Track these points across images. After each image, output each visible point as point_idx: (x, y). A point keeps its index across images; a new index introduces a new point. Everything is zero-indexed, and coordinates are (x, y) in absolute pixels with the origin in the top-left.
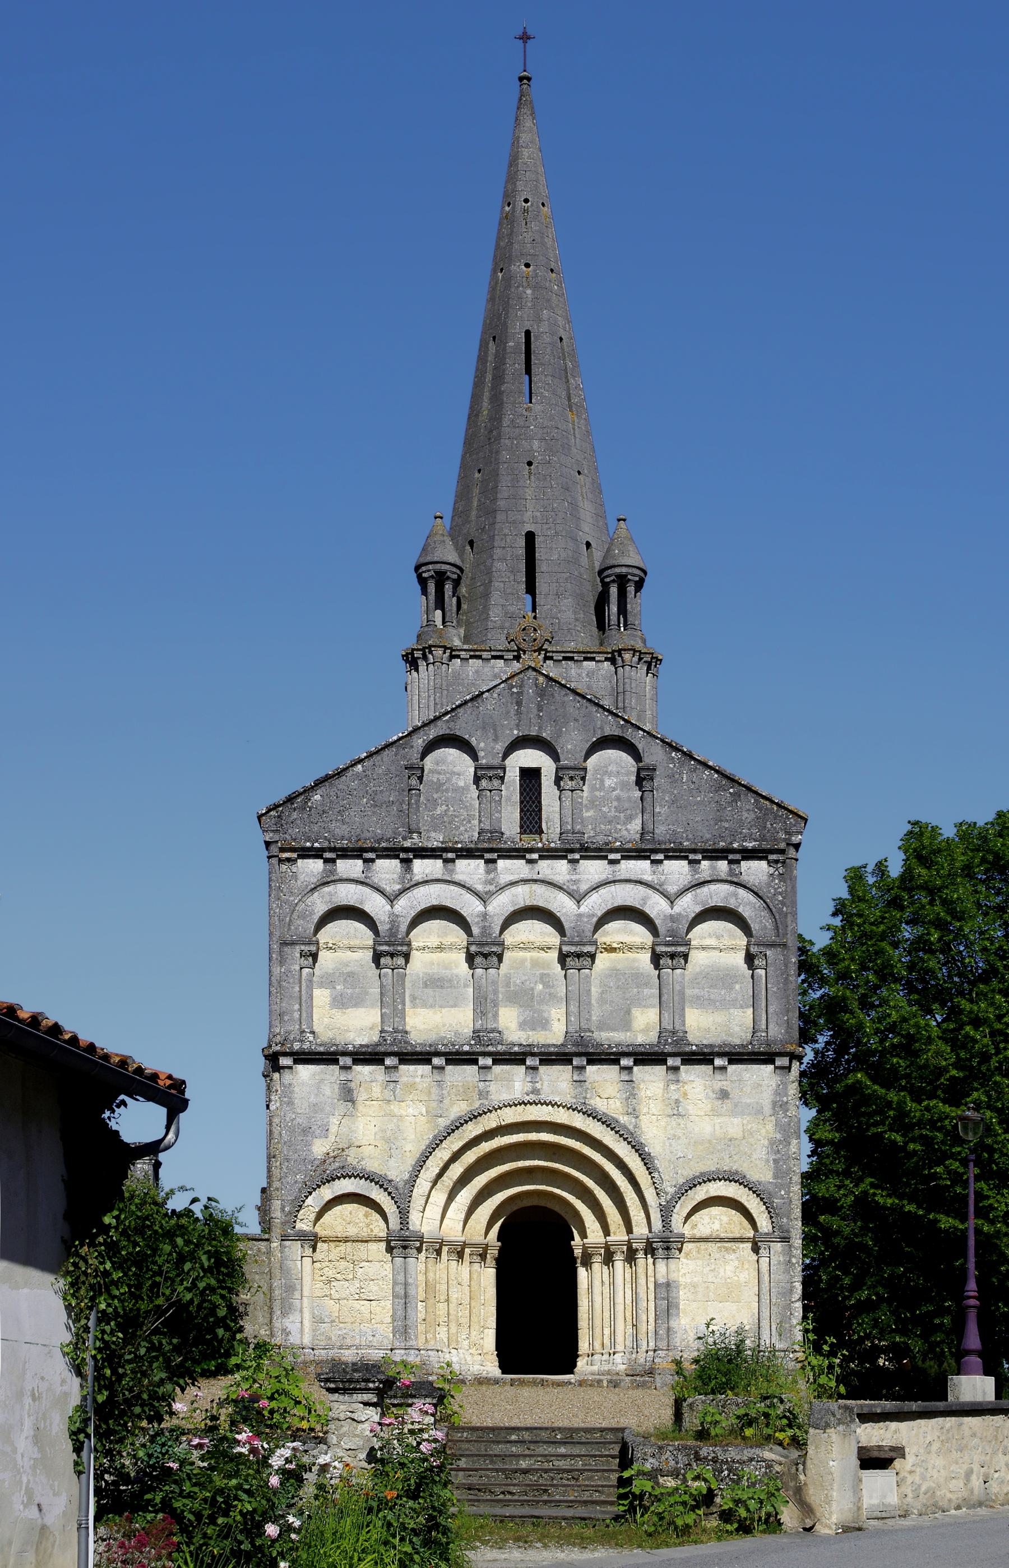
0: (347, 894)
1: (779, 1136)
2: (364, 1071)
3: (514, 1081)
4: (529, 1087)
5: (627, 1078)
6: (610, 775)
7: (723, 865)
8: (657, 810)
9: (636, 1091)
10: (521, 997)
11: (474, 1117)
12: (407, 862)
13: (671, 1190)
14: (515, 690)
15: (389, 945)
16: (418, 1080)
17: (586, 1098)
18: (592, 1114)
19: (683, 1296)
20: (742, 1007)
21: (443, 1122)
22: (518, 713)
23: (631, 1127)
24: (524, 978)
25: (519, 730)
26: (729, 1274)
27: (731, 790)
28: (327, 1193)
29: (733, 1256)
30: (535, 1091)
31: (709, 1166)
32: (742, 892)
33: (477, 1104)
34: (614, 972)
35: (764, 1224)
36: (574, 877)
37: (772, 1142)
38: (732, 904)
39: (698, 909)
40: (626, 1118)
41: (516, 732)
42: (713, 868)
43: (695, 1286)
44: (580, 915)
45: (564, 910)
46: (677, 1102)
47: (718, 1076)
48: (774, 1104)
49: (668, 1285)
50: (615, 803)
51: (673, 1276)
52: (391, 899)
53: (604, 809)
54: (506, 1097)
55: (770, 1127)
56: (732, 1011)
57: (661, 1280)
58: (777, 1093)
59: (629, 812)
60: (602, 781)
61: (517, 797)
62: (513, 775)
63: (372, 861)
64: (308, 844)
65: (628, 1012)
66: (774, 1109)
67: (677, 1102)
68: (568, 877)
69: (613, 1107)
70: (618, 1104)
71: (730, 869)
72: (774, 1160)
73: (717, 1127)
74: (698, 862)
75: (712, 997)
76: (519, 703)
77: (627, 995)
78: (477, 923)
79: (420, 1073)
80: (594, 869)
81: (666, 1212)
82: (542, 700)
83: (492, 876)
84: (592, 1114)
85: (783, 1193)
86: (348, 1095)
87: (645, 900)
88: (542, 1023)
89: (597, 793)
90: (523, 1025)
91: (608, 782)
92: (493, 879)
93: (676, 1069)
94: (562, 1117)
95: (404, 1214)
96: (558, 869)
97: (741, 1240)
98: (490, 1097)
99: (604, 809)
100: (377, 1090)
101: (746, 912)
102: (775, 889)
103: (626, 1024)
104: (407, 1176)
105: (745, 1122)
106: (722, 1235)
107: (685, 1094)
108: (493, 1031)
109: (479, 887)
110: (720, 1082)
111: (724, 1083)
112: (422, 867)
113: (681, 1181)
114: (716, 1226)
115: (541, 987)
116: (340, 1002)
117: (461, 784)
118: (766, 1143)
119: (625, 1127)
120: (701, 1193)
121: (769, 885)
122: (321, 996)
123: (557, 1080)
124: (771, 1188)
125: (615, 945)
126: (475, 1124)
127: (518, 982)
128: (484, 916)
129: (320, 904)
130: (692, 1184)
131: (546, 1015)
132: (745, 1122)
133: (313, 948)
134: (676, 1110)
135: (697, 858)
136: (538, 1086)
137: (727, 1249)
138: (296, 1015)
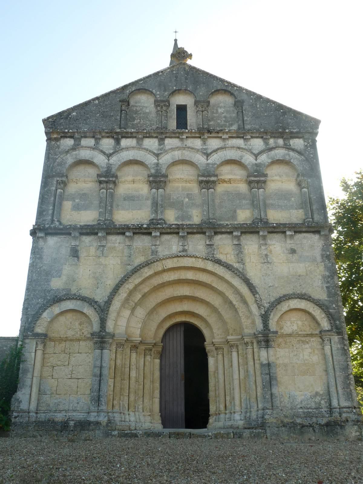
0: (84, 154)
1: (327, 274)
2: (87, 240)
3: (171, 245)
4: (181, 248)
5: (237, 243)
6: (221, 107)
7: (281, 142)
8: (245, 118)
9: (242, 250)
10: (177, 205)
11: (147, 264)
12: (118, 141)
13: (267, 305)
14: (174, 72)
15: (106, 178)
16: (117, 245)
17: (213, 254)
18: (218, 262)
19: (280, 373)
20: (296, 209)
21: (130, 268)
22: (176, 80)
23: (241, 270)
24: (178, 196)
25: (176, 87)
26: (306, 357)
27: (282, 111)
28: (56, 309)
29: (307, 346)
30: (184, 250)
31: (288, 290)
32: (292, 153)
33: (151, 257)
34: (227, 193)
35: (325, 325)
36: (204, 147)
37: (324, 277)
38: (287, 158)
39: (270, 161)
40: (237, 265)
41: (175, 88)
42: (275, 143)
43: (286, 365)
44: (208, 164)
45: (200, 162)
46: (266, 255)
47: (289, 241)
48: (322, 256)
49: (269, 365)
50: (224, 119)
51: (272, 359)
52: (109, 156)
53: (218, 121)
54: (167, 253)
55: (322, 268)
56: (291, 211)
57: (265, 362)
58: (323, 250)
59: (230, 122)
60: (217, 110)
61: (175, 116)
62: (174, 108)
63: (100, 139)
64: (66, 131)
65: (235, 212)
66: (322, 258)
67: (266, 255)
68: (201, 147)
69: (230, 258)
70: (233, 257)
71: (285, 143)
72: (327, 287)
73: (291, 269)
74: (269, 139)
75: (280, 204)
76: (176, 77)
77: (234, 204)
78: (154, 168)
79: (118, 241)
80: (214, 143)
81: (265, 318)
82: (187, 76)
83: (162, 146)
84: (218, 262)
85: (334, 306)
86: (75, 253)
87: (242, 157)
88: (190, 218)
89: (215, 115)
90: (177, 219)
91: (220, 110)
92: (162, 148)
93: (264, 238)
94: (200, 264)
95: (103, 322)
96: (197, 143)
97: (312, 335)
98: (158, 254)
99: (218, 121)
100: (92, 250)
101: (295, 162)
102: (309, 152)
103: (234, 216)
104: (106, 299)
105: (307, 266)
106: (300, 333)
107: (271, 251)
108: (161, 219)
109: (156, 152)
110: (290, 244)
111: (293, 245)
112: (124, 142)
113: (273, 300)
114: (295, 328)
115: (187, 200)
116: (77, 208)
117: (147, 111)
118: (320, 277)
119: (237, 269)
120: (285, 306)
121: (305, 150)
122: (67, 205)
123: (197, 245)
124: (326, 303)
125: (226, 180)
126: (149, 268)
127: (175, 197)
128: (157, 164)
129: (70, 159)
130: (279, 301)
131: (190, 213)
132: (307, 266)
133: (64, 179)
134: (266, 260)
135: (267, 137)
136: (186, 248)
137: (303, 342)
138: (50, 212)
